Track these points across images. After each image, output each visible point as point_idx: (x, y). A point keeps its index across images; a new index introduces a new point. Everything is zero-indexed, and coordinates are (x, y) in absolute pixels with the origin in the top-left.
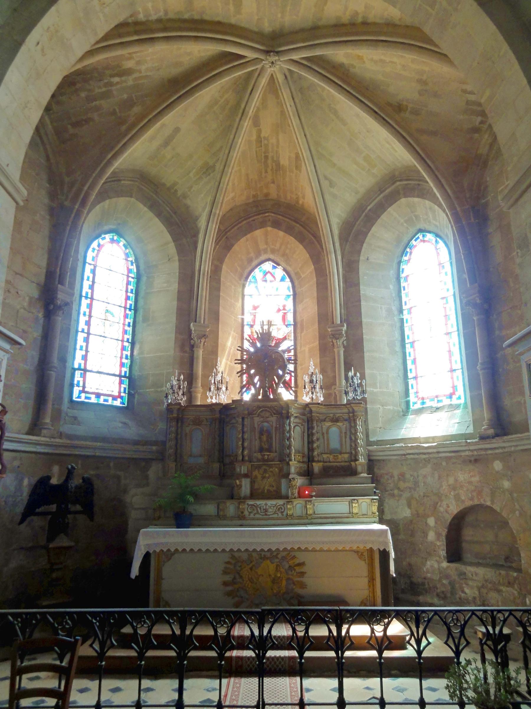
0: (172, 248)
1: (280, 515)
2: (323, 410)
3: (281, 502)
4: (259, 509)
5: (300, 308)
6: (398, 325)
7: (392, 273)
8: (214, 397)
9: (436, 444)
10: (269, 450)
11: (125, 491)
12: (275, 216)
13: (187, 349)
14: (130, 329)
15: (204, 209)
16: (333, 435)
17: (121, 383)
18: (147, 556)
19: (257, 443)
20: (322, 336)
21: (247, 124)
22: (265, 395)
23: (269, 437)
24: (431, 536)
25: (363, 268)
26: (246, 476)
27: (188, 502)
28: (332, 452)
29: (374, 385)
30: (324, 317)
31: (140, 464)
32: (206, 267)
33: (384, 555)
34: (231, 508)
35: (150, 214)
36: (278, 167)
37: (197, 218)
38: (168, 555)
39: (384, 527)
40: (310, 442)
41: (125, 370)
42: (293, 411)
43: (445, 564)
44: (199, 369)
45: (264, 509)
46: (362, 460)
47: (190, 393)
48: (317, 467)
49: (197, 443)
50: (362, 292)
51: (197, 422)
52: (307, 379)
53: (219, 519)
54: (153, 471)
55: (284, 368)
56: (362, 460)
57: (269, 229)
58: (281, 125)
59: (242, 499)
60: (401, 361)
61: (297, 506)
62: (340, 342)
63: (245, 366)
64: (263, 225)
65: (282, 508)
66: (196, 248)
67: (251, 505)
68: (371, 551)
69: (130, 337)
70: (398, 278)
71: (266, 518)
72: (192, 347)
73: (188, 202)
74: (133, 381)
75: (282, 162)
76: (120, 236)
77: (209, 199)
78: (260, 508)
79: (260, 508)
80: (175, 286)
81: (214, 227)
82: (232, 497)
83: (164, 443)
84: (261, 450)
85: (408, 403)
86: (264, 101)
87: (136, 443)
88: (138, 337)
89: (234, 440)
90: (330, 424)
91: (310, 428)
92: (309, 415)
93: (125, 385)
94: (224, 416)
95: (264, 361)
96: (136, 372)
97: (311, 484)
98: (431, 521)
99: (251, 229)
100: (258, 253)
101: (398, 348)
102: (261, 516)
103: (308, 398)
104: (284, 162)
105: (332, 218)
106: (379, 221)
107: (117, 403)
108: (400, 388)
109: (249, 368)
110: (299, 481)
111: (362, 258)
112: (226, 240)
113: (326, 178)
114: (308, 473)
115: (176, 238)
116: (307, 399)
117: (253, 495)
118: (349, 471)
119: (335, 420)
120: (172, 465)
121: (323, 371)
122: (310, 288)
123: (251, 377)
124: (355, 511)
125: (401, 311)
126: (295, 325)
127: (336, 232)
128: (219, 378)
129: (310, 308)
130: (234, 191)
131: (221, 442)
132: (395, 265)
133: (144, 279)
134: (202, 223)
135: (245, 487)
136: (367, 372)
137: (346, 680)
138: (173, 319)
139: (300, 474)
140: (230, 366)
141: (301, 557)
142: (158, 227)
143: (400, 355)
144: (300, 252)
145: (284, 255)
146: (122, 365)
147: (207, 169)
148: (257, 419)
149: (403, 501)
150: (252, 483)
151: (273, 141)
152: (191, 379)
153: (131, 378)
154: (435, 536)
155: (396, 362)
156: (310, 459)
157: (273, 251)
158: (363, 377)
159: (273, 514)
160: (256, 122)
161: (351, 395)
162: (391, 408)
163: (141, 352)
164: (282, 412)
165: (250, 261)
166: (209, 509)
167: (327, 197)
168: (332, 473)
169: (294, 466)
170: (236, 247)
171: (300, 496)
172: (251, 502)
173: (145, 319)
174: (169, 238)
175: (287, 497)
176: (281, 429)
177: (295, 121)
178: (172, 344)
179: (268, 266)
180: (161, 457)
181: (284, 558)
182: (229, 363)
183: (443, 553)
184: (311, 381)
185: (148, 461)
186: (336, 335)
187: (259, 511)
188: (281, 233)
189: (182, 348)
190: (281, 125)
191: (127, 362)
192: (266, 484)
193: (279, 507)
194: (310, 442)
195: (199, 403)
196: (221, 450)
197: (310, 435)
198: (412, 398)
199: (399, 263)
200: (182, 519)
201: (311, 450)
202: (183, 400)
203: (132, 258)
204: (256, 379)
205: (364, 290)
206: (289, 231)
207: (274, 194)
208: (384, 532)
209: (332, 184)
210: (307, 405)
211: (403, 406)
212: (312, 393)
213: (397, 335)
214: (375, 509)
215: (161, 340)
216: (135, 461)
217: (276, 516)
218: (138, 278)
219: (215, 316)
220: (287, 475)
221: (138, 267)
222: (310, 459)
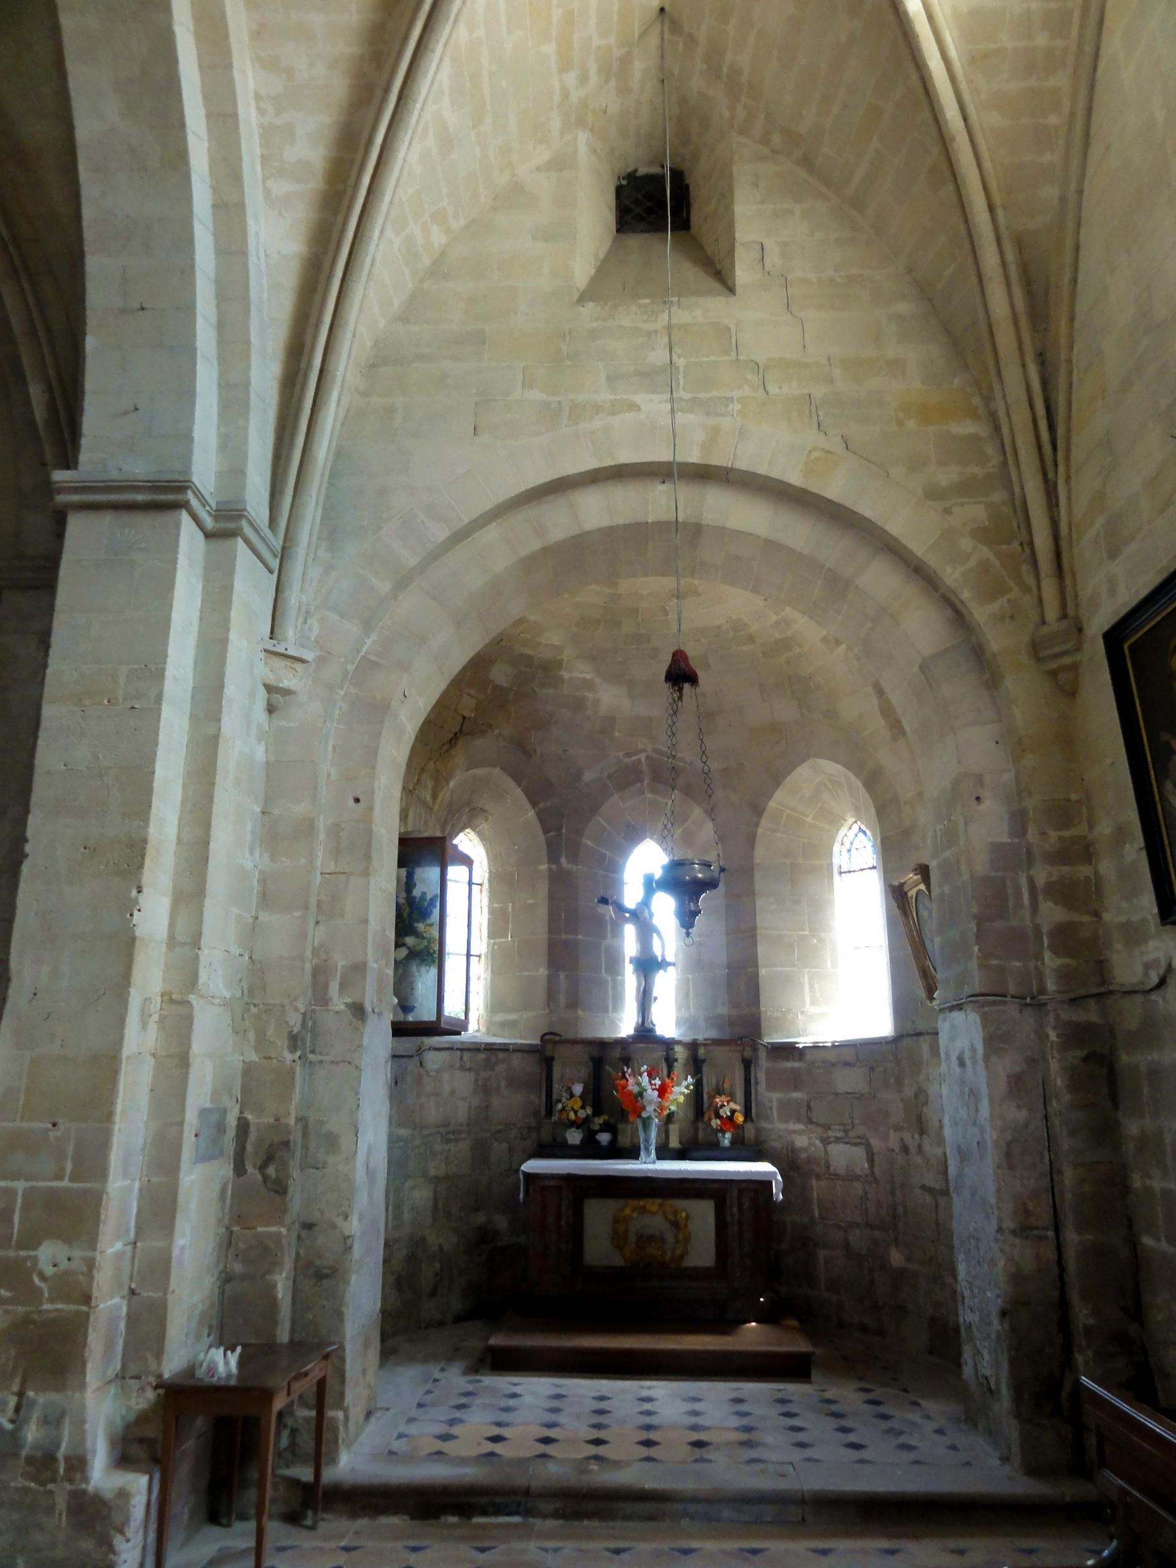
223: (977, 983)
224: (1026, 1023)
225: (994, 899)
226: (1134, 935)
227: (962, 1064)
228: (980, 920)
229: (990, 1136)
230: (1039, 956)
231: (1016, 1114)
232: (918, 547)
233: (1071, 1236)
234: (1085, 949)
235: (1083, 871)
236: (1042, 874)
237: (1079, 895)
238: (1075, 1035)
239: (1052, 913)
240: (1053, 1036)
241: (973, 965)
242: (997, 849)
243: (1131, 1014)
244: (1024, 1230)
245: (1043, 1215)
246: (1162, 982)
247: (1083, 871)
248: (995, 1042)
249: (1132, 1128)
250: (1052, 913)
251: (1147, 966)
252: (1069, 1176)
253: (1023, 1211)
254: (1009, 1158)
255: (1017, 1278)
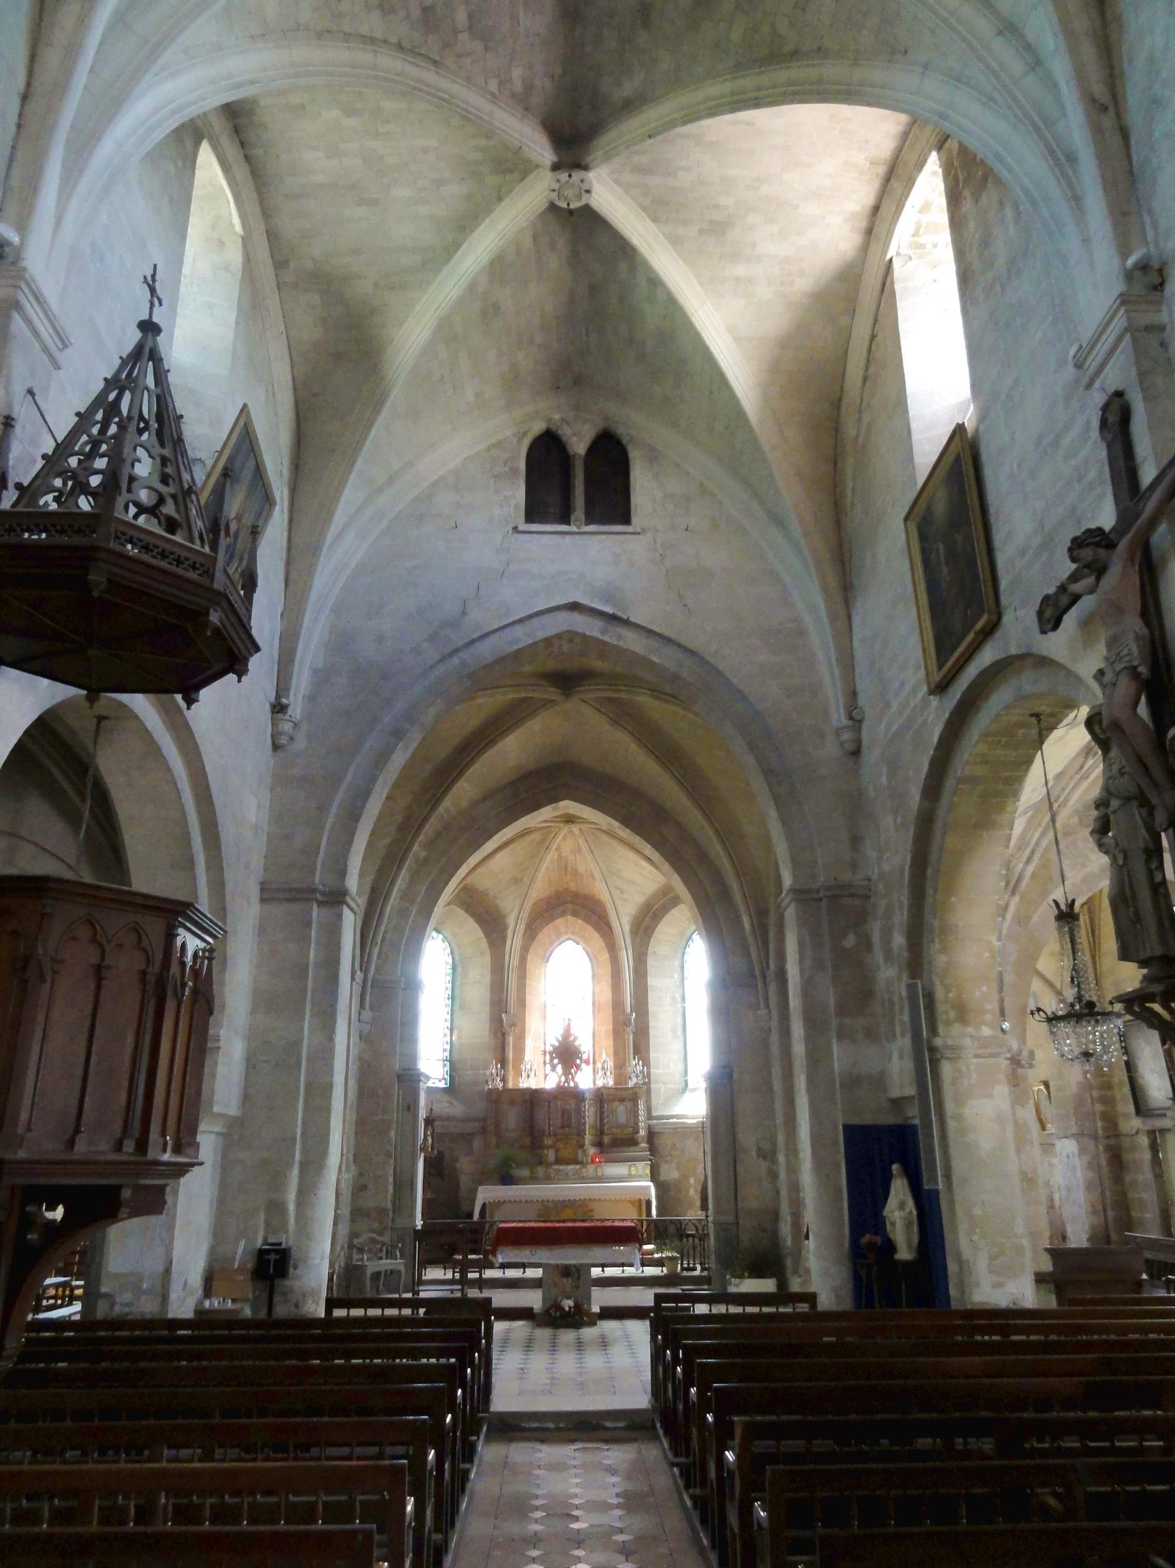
0: (484, 943)
2: (613, 1092)
3: (578, 1167)
5: (597, 991)
6: (681, 1011)
7: (677, 963)
9: (695, 1121)
10: (569, 1126)
11: (457, 1160)
12: (575, 906)
13: (499, 1035)
14: (449, 1017)
15: (513, 910)
16: (621, 1112)
17: (445, 1065)
18: (484, 1206)
19: (559, 1122)
20: (615, 1021)
21: (549, 857)
22: (566, 1081)
23: (569, 1117)
24: (692, 1192)
25: (651, 962)
26: (551, 1147)
27: (510, 1167)
28: (618, 1127)
29: (658, 1067)
30: (617, 1004)
31: (467, 1138)
32: (515, 962)
33: (649, 1203)
34: (541, 1171)
35: (466, 915)
36: (575, 873)
37: (505, 917)
38: (499, 1204)
39: (651, 1184)
40: (602, 1119)
41: (447, 1054)
42: (587, 1095)
43: (699, 1212)
44: (510, 1055)
46: (642, 1133)
47: (504, 1080)
48: (606, 1139)
49: (512, 1119)
50: (649, 983)
51: (512, 1102)
52: (599, 1065)
53: (533, 1179)
54: (477, 1143)
55: (581, 1059)
56: (642, 1133)
57: (569, 917)
58: (577, 851)
59: (549, 1165)
60: (682, 1044)
61: (591, 1168)
62: (629, 1030)
63: (548, 1057)
64: (563, 914)
66: (505, 942)
68: (640, 1200)
69: (449, 1024)
70: (682, 968)
71: (566, 1178)
72: (504, 1034)
73: (498, 902)
74: (454, 1066)
75: (579, 870)
76: (439, 932)
77: (517, 904)
80: (488, 978)
81: (522, 927)
82: (541, 1163)
83: (484, 1120)
84: (563, 1127)
85: (686, 1082)
86: (564, 838)
87: (463, 1120)
88: (456, 1023)
89: (541, 1115)
90: (617, 1103)
91: (602, 1108)
92: (601, 1097)
93: (447, 1068)
94: (533, 1098)
95: (567, 1055)
96: (456, 1056)
97: (602, 1152)
98: (692, 1181)
99: (552, 919)
100: (559, 935)
101: (680, 1032)
104: (581, 869)
105: (622, 919)
106: (664, 920)
107: (442, 1085)
108: (681, 1067)
109: (552, 1059)
110: (592, 1151)
111: (650, 951)
112: (531, 932)
113: (616, 887)
114: (599, 1144)
115: (488, 935)
116: (600, 1083)
117: (558, 1161)
118: (632, 1142)
119: (622, 1100)
120: (493, 1140)
121: (616, 1053)
122: (606, 971)
123: (554, 1068)
124: (633, 1173)
125: (683, 999)
126: (594, 1004)
127: (627, 928)
128: (528, 1067)
129: (606, 995)
130: (539, 890)
131: (532, 1119)
132: (679, 956)
133: (459, 969)
134: (511, 921)
135: (551, 1155)
136: (652, 1055)
137: (640, 1331)
138: (487, 1008)
139: (593, 1145)
141: (593, 1205)
142: (472, 925)
143: (681, 1038)
144: (597, 939)
145: (583, 937)
146: (445, 1050)
147: (517, 880)
148: (559, 1103)
149: (674, 1165)
150: (557, 1151)
151: (571, 858)
152: (503, 1062)
153: (451, 1061)
154: (694, 1194)
155: (677, 1046)
156: (602, 1133)
157: (573, 933)
158: (646, 1063)
160: (558, 849)
161: (635, 1080)
162: (671, 1086)
163: (460, 1037)
164: (577, 1096)
165: (552, 943)
166: (525, 1172)
167: (619, 903)
168: (617, 1143)
169: (588, 1138)
170: (540, 936)
171: (593, 1162)
172: (556, 1167)
173: (462, 1008)
174: (482, 935)
175: (581, 1163)
176: (579, 1112)
177: (589, 857)
178: (487, 1032)
179: (569, 944)
180: (483, 1131)
181: (580, 1206)
183: (698, 1204)
184: (603, 1068)
185: (472, 1135)
186: (627, 1023)
188: (580, 922)
189: (495, 1034)
190: (577, 851)
191: (448, 1047)
192: (566, 1153)
194: (602, 1119)
195: (510, 1085)
196: (532, 1126)
197: (602, 1113)
198: (689, 1078)
199: (684, 953)
200: (507, 1179)
201: (602, 1125)
202: (500, 1085)
203: (449, 951)
204: (560, 1066)
205: (652, 981)
206: (587, 920)
207: (573, 887)
208: (648, 1188)
209: (622, 892)
210: (599, 1089)
211: (683, 1084)
213: (680, 1020)
214: (648, 1171)
215: (476, 1027)
216: (462, 1135)
218: (454, 968)
219: (522, 1003)
220: (582, 1146)
221: (453, 959)
222: (602, 1133)
223: (1074, 1130)
224: (1090, 1144)
225: (1079, 1101)
226: (1127, 1116)
227: (1068, 1157)
228: (1076, 1108)
229: (1081, 1182)
230: (1095, 1121)
231: (1090, 1174)
232: (1049, 976)
233: (1110, 1213)
234: (1111, 1121)
235: (1109, 1093)
236: (1095, 1094)
237: (1108, 1101)
238: (1109, 1149)
239: (1099, 1108)
240: (1101, 1148)
241: (1073, 1123)
242: (1079, 1083)
243: (1126, 1143)
244: (1094, 1213)
245: (1100, 1208)
246: (1137, 1133)
247: (1109, 1093)
248: (1082, 1150)
249: (1128, 1178)
250: (1099, 1108)
251: (1132, 1127)
252: (1108, 1193)
253: (1093, 1206)
254: (1089, 1186)
255: (1093, 1227)
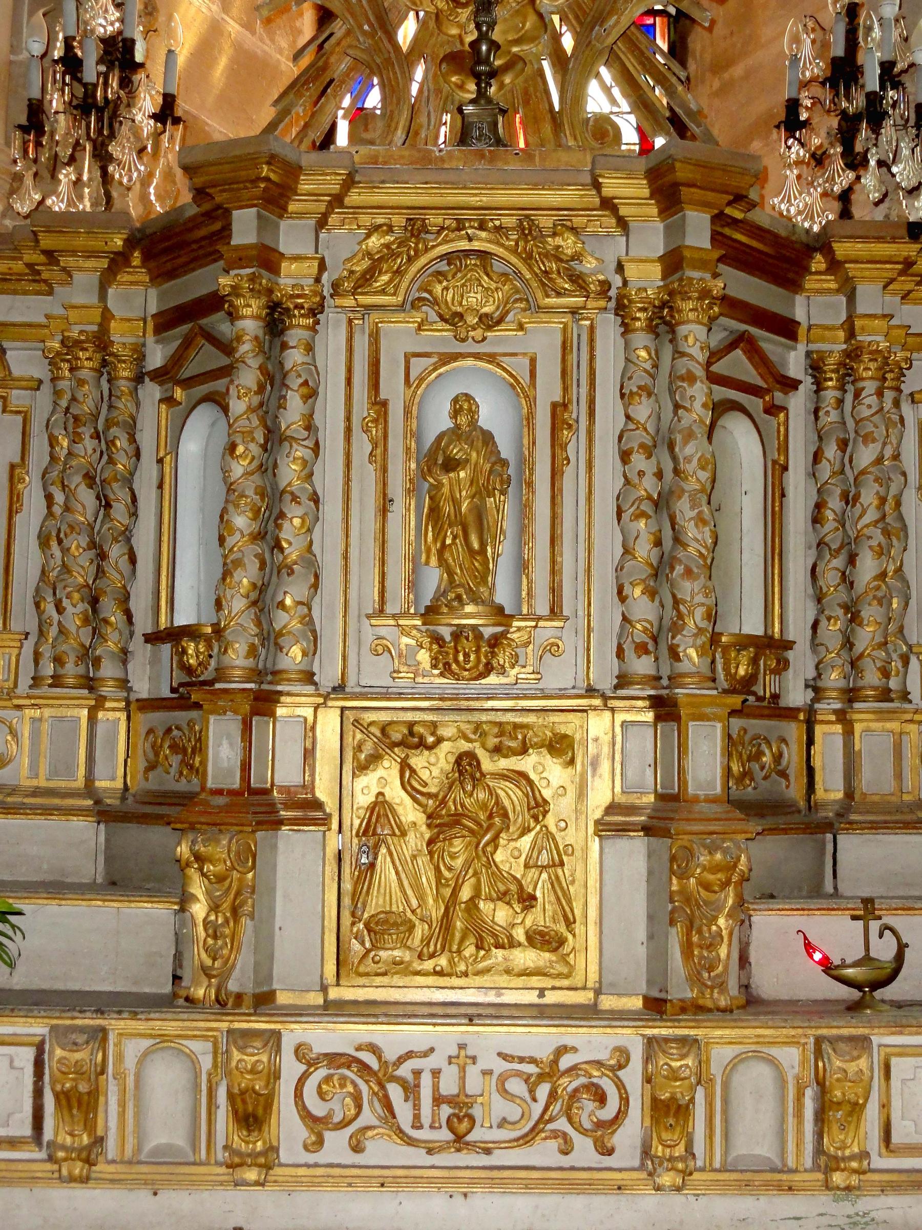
1: (584, 1151)
4: (395, 1092)
8: (66, 175)
45: (438, 1100)
65: (601, 1098)
67: (333, 1059)
78: (411, 1090)
79: (411, 1090)
102: (418, 1156)
103: (813, 198)
140: (238, 48)
159: (526, 1139)
182: (233, 27)
187: (403, 1112)
193: (568, 1084)
212: (855, 162)
217: (544, 1153)
